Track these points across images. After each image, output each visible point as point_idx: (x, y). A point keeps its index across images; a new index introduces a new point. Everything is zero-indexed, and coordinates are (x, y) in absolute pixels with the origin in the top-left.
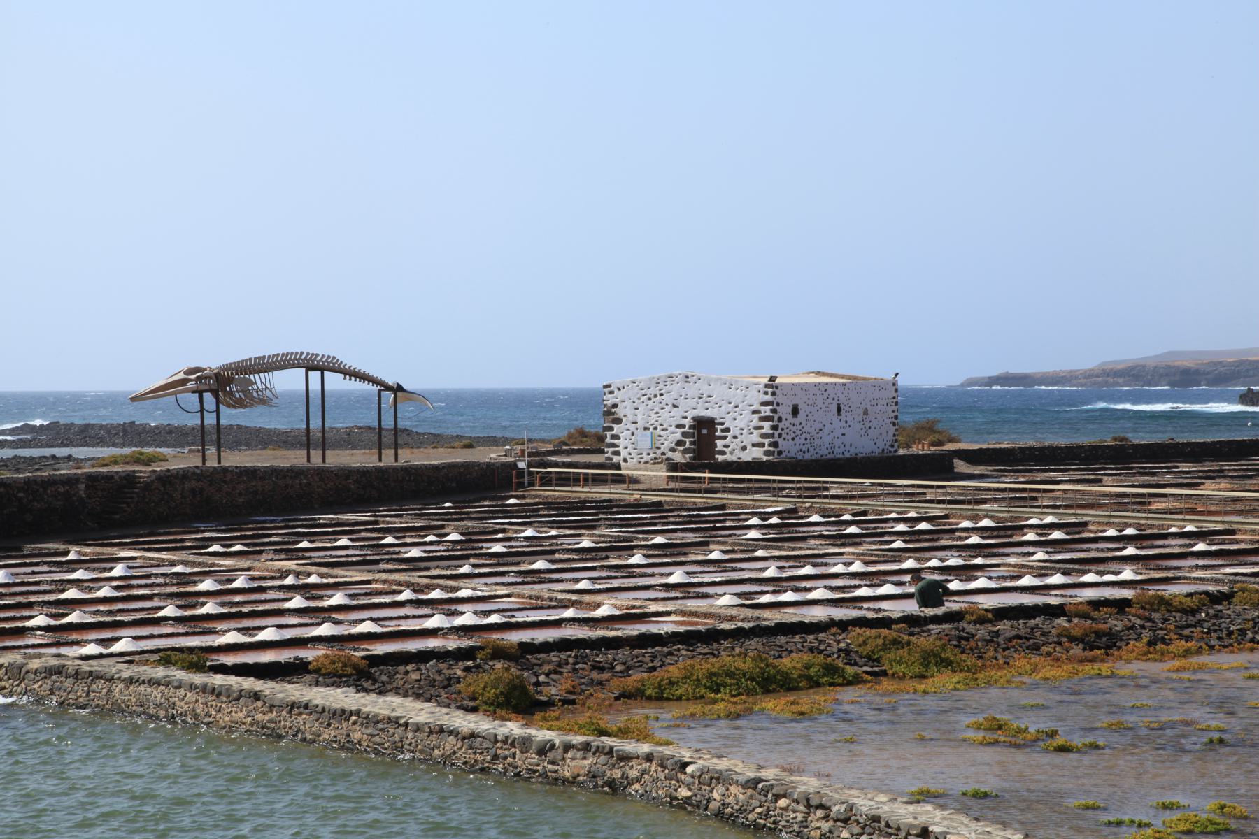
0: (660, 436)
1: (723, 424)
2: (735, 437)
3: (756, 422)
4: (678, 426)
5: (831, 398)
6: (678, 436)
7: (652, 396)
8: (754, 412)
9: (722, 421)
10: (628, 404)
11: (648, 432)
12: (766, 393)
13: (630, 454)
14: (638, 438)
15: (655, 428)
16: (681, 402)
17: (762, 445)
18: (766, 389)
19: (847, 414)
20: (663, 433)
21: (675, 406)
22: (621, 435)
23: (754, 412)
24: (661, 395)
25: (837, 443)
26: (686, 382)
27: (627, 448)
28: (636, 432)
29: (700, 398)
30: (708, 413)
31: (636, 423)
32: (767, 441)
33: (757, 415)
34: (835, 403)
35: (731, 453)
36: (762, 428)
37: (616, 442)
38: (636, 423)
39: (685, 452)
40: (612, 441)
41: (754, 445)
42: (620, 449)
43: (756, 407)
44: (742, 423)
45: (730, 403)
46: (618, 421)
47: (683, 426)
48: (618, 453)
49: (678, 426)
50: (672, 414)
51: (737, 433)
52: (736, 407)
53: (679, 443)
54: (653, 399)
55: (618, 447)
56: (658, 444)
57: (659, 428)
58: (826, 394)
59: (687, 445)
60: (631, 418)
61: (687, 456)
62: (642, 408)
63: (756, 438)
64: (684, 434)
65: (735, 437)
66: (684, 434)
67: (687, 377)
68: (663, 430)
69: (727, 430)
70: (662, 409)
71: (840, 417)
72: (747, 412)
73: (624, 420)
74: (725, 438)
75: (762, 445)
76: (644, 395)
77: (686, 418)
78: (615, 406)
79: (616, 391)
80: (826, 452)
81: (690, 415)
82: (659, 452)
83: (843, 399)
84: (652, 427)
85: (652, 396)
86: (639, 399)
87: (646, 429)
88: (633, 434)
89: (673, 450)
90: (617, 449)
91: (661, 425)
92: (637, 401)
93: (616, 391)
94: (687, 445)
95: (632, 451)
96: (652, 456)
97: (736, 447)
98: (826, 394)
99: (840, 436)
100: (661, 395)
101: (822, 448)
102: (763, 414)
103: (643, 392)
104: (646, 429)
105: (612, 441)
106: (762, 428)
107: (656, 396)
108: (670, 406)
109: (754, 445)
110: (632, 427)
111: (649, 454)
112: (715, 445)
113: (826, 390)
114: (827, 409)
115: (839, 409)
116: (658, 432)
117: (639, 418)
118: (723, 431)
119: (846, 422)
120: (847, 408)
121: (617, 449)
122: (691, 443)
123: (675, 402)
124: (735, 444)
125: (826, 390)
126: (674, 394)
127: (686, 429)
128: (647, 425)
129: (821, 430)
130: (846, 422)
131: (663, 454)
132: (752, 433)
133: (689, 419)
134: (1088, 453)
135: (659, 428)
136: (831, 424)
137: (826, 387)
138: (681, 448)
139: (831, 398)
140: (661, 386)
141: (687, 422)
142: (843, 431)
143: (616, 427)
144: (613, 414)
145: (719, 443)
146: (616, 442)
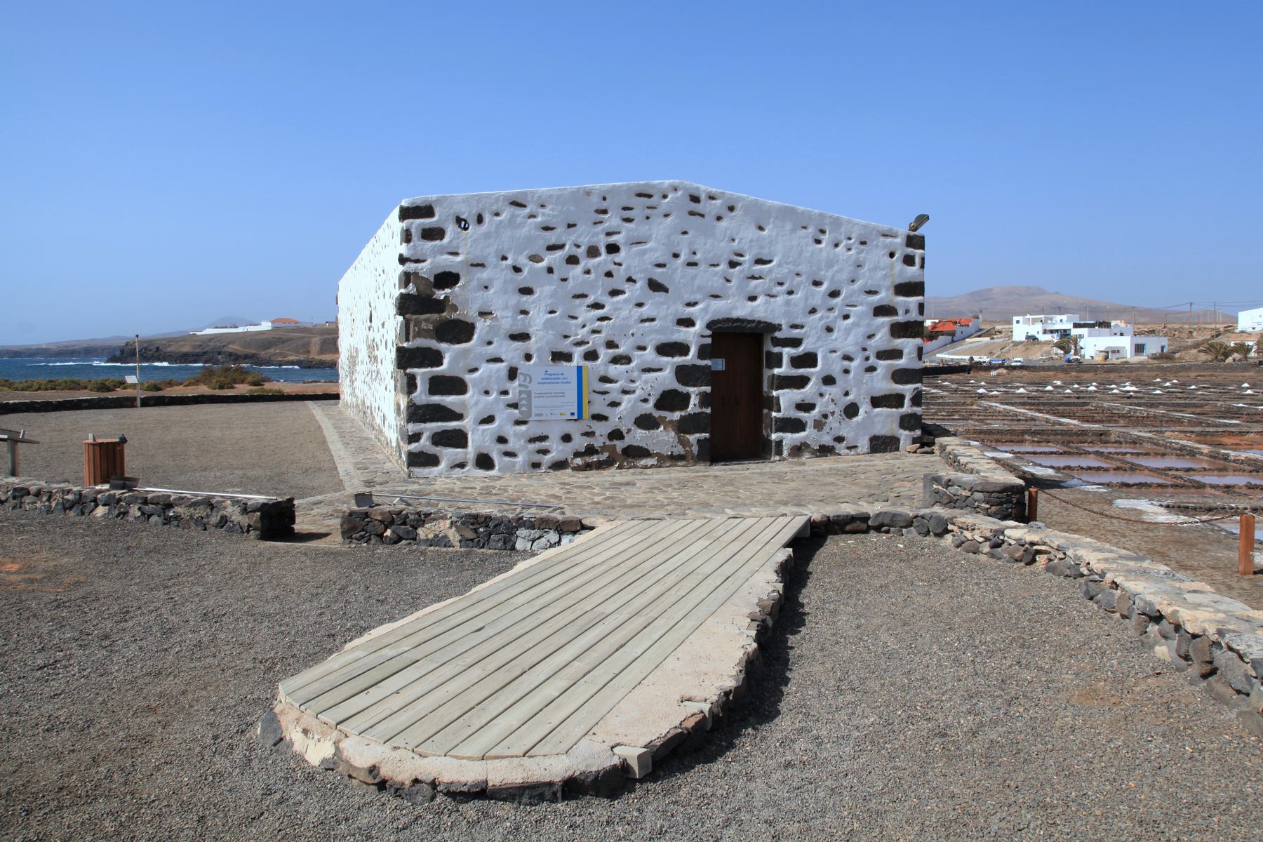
0: (605, 379)
1: (796, 342)
2: (829, 380)
3: (883, 339)
4: (667, 349)
6: (666, 379)
7: (581, 252)
8: (881, 311)
9: (796, 333)
10: (497, 274)
11: (569, 368)
12: (909, 260)
13: (502, 440)
14: (534, 387)
15: (591, 356)
16: (675, 274)
17: (896, 400)
18: (910, 250)
20: (615, 370)
21: (655, 286)
22: (468, 378)
23: (881, 311)
24: (613, 249)
26: (692, 213)
27: (489, 420)
28: (523, 366)
29: (733, 264)
30: (745, 311)
31: (523, 337)
32: (908, 389)
33: (885, 320)
35: (819, 425)
36: (896, 354)
37: (449, 400)
38: (523, 337)
39: (684, 427)
40: (437, 399)
41: (876, 402)
42: (467, 424)
43: (885, 296)
44: (847, 338)
45: (817, 283)
46: (460, 331)
47: (682, 349)
48: (457, 439)
49: (667, 349)
50: (645, 311)
51: (836, 370)
52: (834, 294)
53: (670, 400)
54: (585, 263)
55: (459, 417)
56: (600, 406)
57: (605, 354)
59: (693, 406)
60: (506, 320)
61: (693, 438)
62: (545, 291)
63: (882, 383)
64: (684, 374)
65: (829, 380)
66: (684, 374)
67: (695, 199)
68: (616, 360)
69: (809, 360)
70: (615, 293)
72: (862, 308)
73: (481, 326)
74: (801, 382)
75: (896, 400)
76: (551, 248)
77: (688, 322)
78: (447, 279)
79: (451, 230)
81: (703, 314)
82: (602, 429)
84: (578, 353)
85: (581, 252)
86: (535, 258)
87: (561, 357)
88: (513, 374)
89: (646, 422)
90: (453, 424)
91: (611, 345)
92: (528, 266)
93: (451, 230)
94: (693, 406)
95: (511, 431)
96: (580, 443)
97: (832, 407)
100: (613, 249)
102: (900, 318)
103: (552, 238)
104: (561, 357)
105: (437, 399)
106: (896, 354)
107: (593, 252)
108: (641, 284)
109: (876, 402)
110: (511, 352)
111: (567, 438)
112: (774, 404)
116: (601, 365)
117: (537, 322)
118: (797, 362)
121: (453, 424)
122: (705, 400)
123: (658, 275)
124: (828, 401)
126: (655, 249)
127: (691, 358)
128: (565, 346)
131: (616, 435)
132: (872, 369)
133: (699, 326)
135: (605, 354)
138: (677, 415)
140: (612, 221)
141: (693, 336)
143: (450, 352)
144: (440, 306)
145: (787, 398)
146: (449, 400)
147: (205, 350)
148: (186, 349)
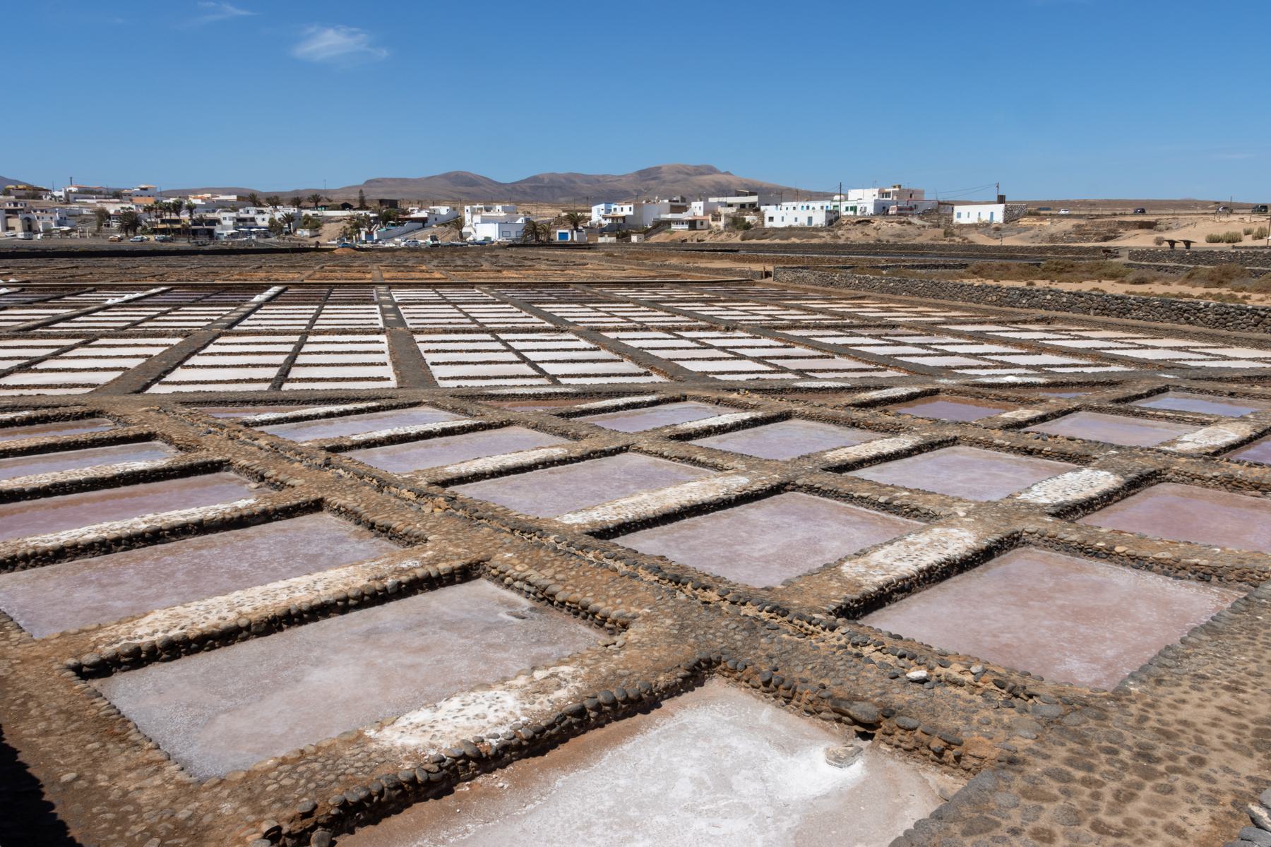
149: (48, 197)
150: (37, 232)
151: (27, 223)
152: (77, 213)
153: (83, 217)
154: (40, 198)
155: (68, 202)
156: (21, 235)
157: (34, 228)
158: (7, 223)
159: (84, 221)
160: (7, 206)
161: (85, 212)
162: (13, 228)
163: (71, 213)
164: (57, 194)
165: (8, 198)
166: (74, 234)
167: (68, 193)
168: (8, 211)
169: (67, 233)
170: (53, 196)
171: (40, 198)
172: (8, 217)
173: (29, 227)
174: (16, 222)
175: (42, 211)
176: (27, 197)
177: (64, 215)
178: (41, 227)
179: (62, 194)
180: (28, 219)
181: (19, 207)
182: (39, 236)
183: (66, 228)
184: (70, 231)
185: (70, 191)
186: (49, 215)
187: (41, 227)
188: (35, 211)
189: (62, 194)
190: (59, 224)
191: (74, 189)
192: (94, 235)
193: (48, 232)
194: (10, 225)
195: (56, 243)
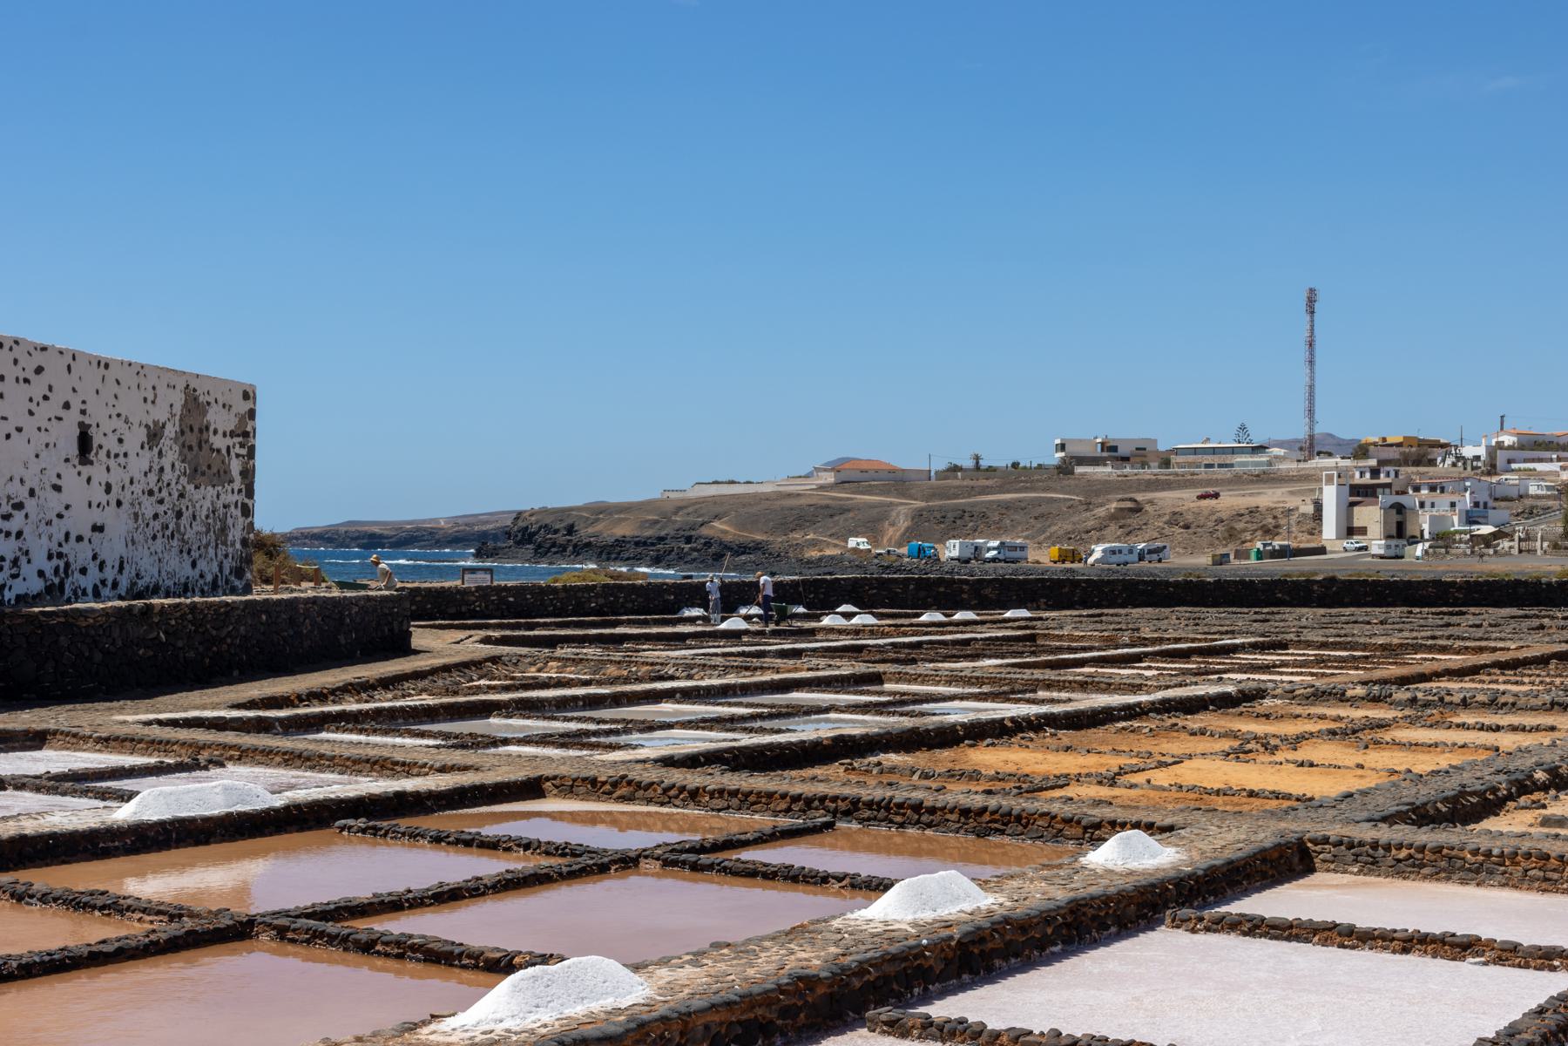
5: (57, 399)
19: (112, 463)
25: (80, 554)
34: (73, 417)
58: (38, 387)
71: (86, 470)
80: (36, 585)
83: (98, 415)
98: (38, 387)
99: (87, 533)
101: (25, 569)
113: (39, 370)
114: (44, 438)
115: (85, 443)
119: (108, 489)
120: (111, 444)
125: (39, 370)
129: (19, 506)
130: (108, 489)
134: (601, 601)
136: (57, 488)
137: (39, 358)
139: (57, 399)
142: (97, 517)
147: (663, 534)
148: (623, 530)
149: (1449, 461)
150: (1414, 540)
151: (1395, 517)
152: (1514, 494)
153: (1528, 502)
154: (1432, 463)
155: (1492, 469)
156: (1377, 546)
157: (1411, 530)
158: (1350, 517)
159: (1530, 513)
160: (1357, 479)
161: (1533, 490)
162: (1363, 531)
163: (1500, 492)
164: (1468, 451)
165: (1362, 463)
166: (1505, 544)
167: (1492, 451)
168: (1356, 490)
169: (1487, 541)
170: (1459, 458)
171: (1432, 463)
172: (1353, 504)
173: (1399, 530)
174: (1371, 516)
175: (1433, 489)
176: (1405, 461)
177: (1483, 497)
178: (1426, 527)
179: (1481, 451)
180: (1399, 508)
181: (1383, 479)
182: (1419, 549)
183: (1486, 529)
184: (1496, 536)
185: (1500, 445)
186: (1449, 497)
187: (1426, 527)
188: (1417, 489)
189: (1481, 451)
190: (1471, 519)
191: (1508, 440)
192: (1555, 546)
193: (1443, 540)
194: (1357, 523)
195: (1460, 566)
